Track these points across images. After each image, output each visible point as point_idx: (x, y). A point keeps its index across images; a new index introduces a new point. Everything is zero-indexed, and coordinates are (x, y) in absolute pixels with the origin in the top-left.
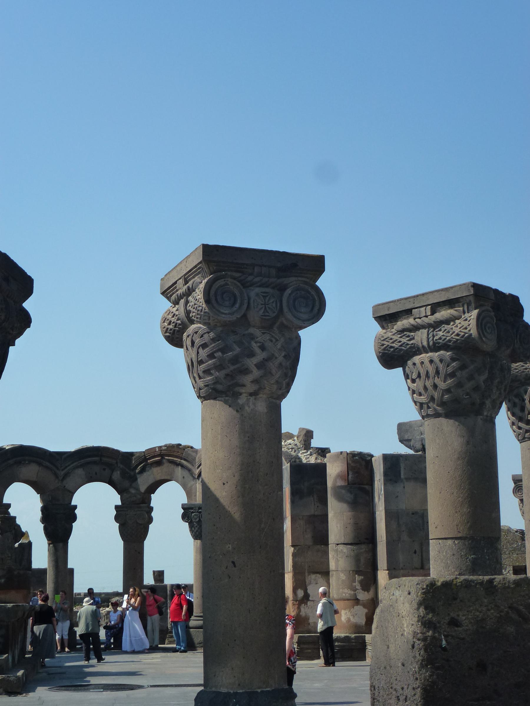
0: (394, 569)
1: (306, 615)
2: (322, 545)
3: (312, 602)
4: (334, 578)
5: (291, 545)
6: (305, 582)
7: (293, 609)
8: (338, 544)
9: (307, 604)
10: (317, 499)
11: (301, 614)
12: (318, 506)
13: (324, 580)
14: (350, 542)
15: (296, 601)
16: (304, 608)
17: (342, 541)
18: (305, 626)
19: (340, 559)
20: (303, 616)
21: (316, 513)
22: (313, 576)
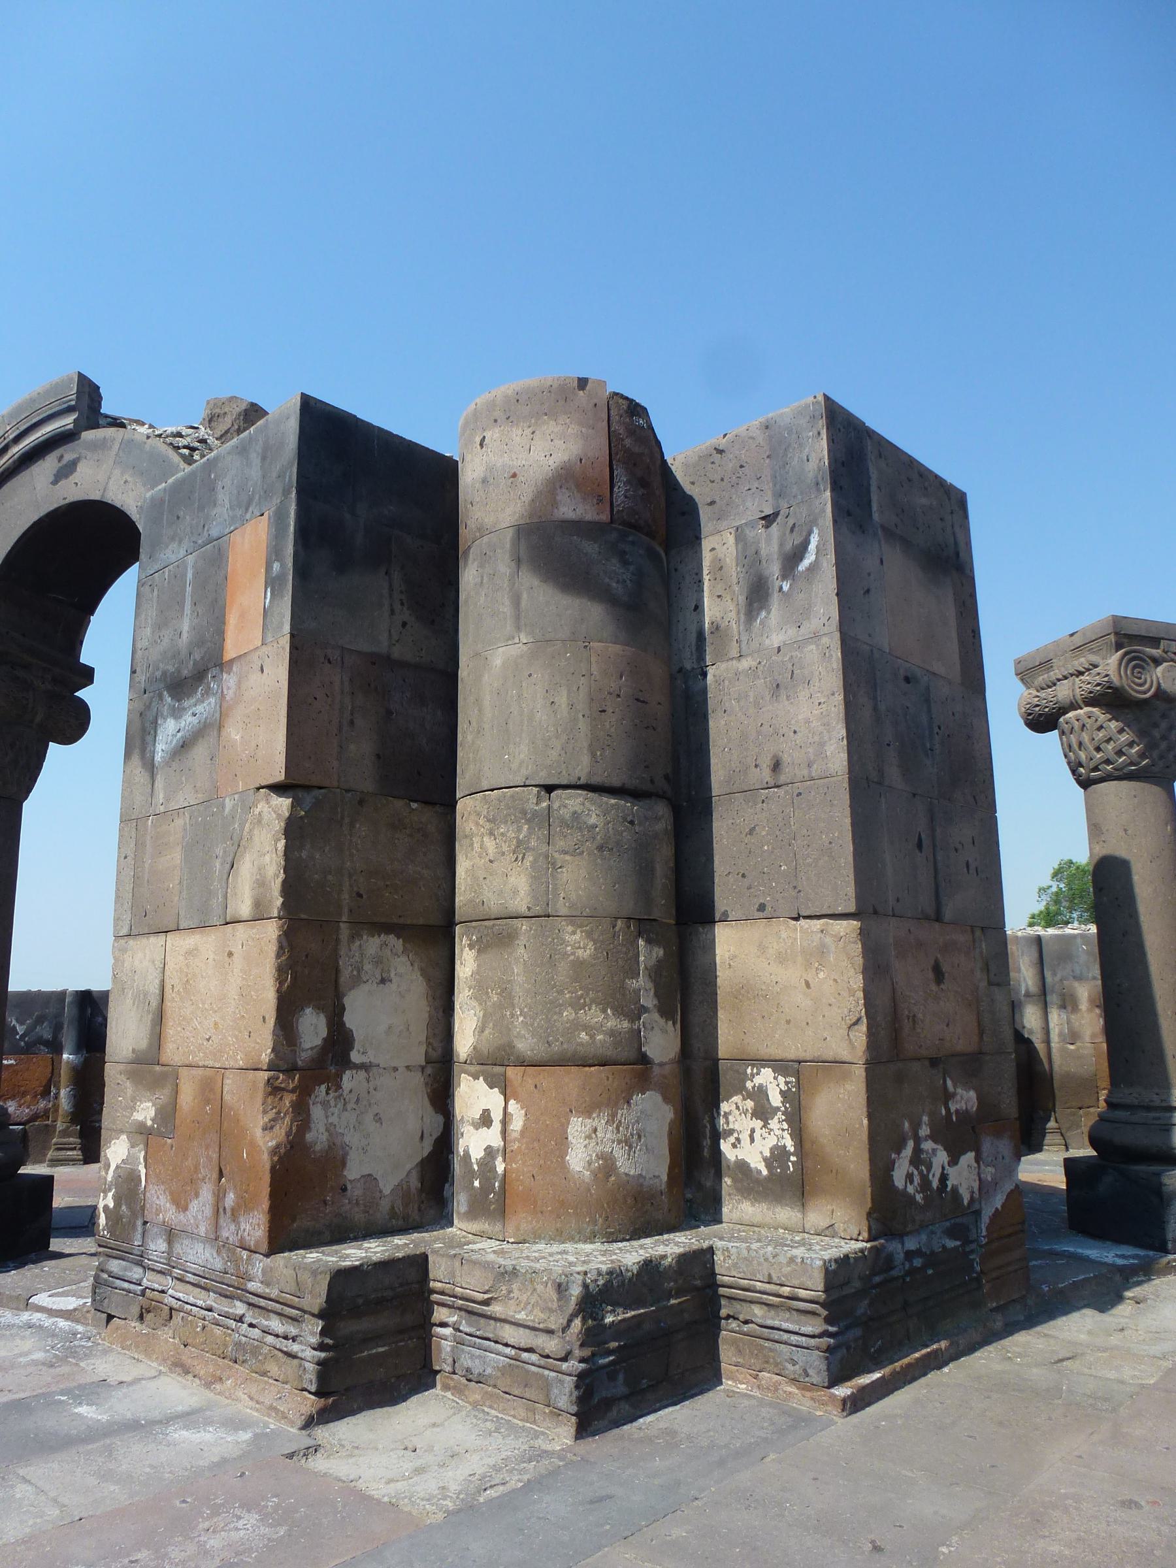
0: (875, 912)
1: (332, 1146)
2: (415, 801)
3: (362, 1074)
4: (521, 950)
5: (279, 776)
6: (337, 971)
7: (265, 1112)
8: (549, 789)
9: (339, 1087)
10: (401, 592)
11: (309, 1137)
12: (404, 624)
13: (416, 965)
14: (616, 781)
15: (290, 1070)
16: (325, 1105)
17: (582, 770)
18: (325, 1203)
19: (568, 857)
20: (318, 1148)
21: (396, 653)
22: (372, 944)
